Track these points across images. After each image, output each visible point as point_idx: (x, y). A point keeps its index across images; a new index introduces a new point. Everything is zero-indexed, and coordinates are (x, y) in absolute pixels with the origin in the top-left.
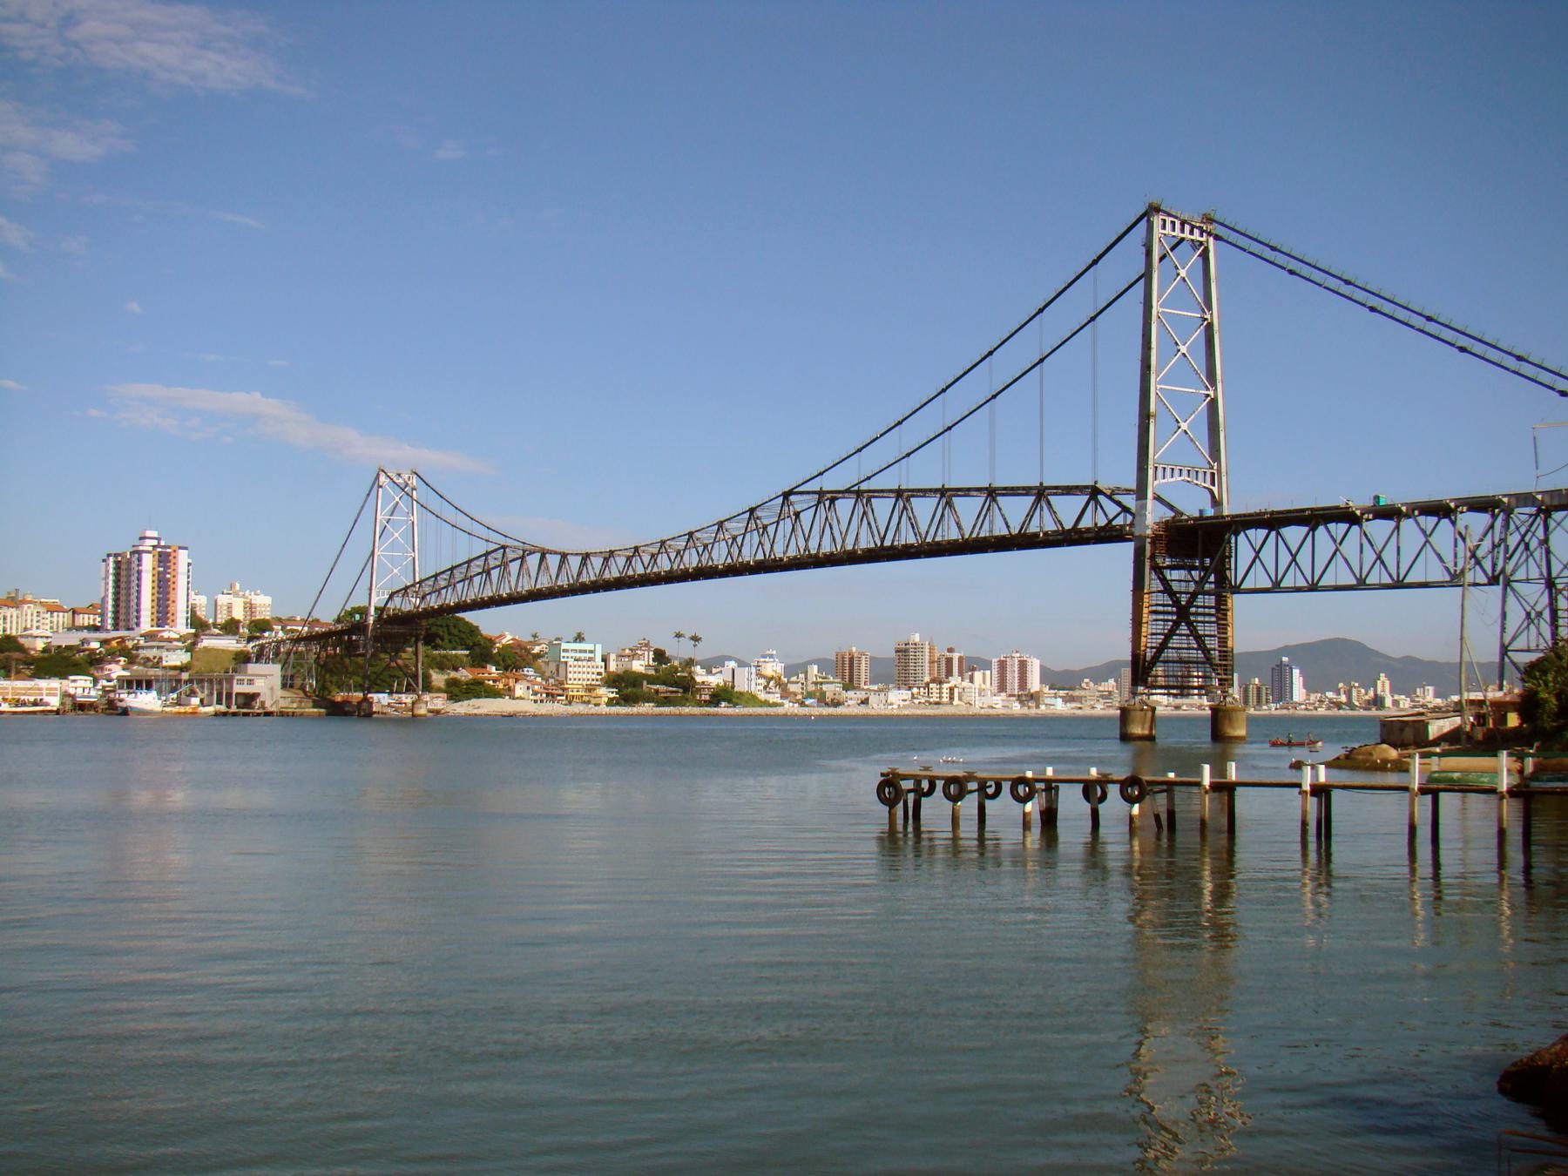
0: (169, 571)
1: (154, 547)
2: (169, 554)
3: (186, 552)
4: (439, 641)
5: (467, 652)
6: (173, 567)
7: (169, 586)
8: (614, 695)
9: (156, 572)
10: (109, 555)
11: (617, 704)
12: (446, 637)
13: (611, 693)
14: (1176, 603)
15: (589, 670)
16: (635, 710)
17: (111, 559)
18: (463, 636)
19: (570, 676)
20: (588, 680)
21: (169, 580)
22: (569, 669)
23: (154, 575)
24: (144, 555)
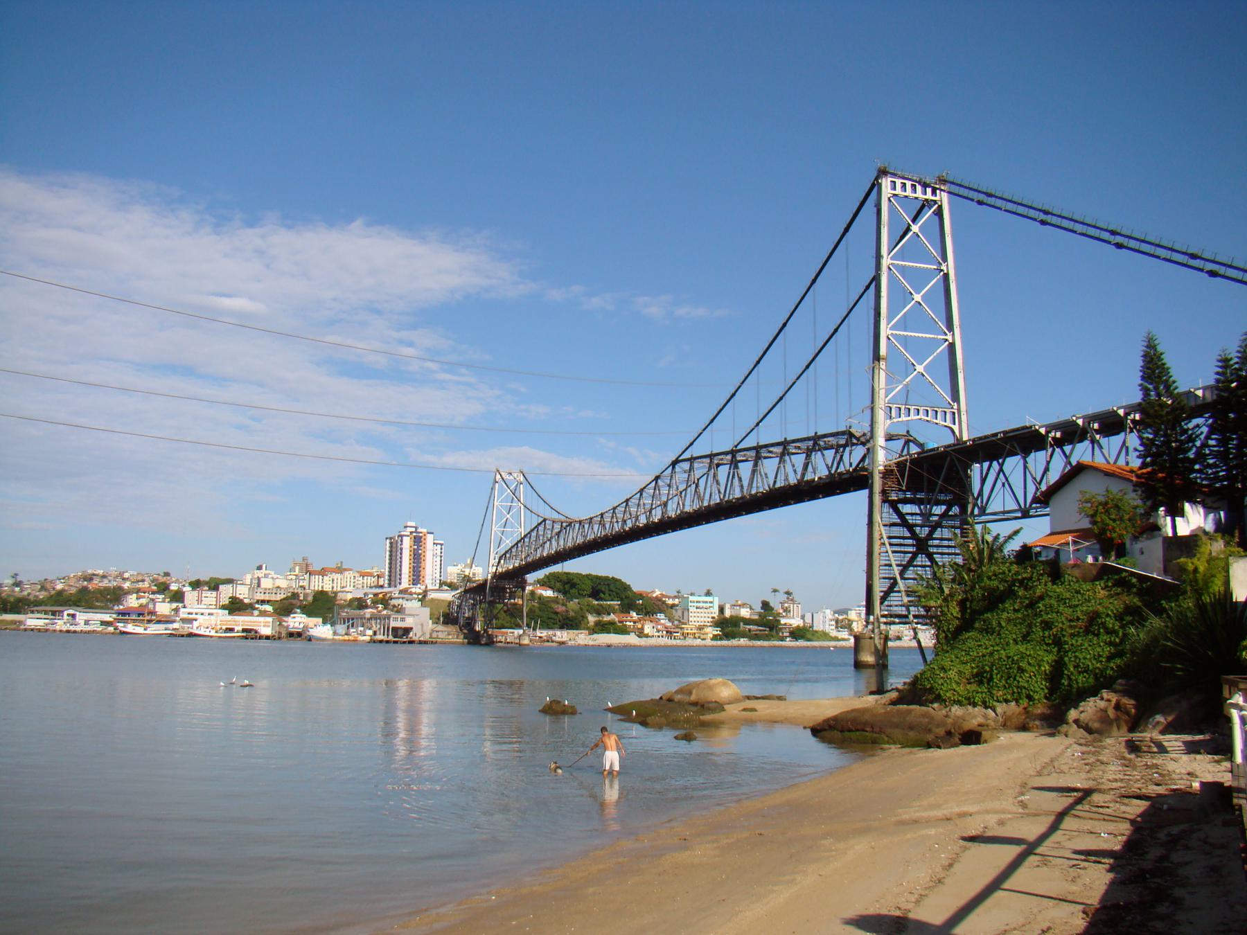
1: (411, 533)
2: (421, 537)
3: (432, 535)
4: (602, 595)
5: (619, 602)
6: (423, 545)
7: (421, 559)
8: (718, 632)
9: (412, 549)
10: (387, 539)
11: (721, 639)
12: (607, 592)
13: (717, 631)
15: (705, 615)
16: (734, 642)
17: (388, 541)
18: (619, 591)
19: (691, 619)
20: (705, 622)
21: (421, 554)
22: (690, 614)
23: (411, 551)
24: (404, 538)
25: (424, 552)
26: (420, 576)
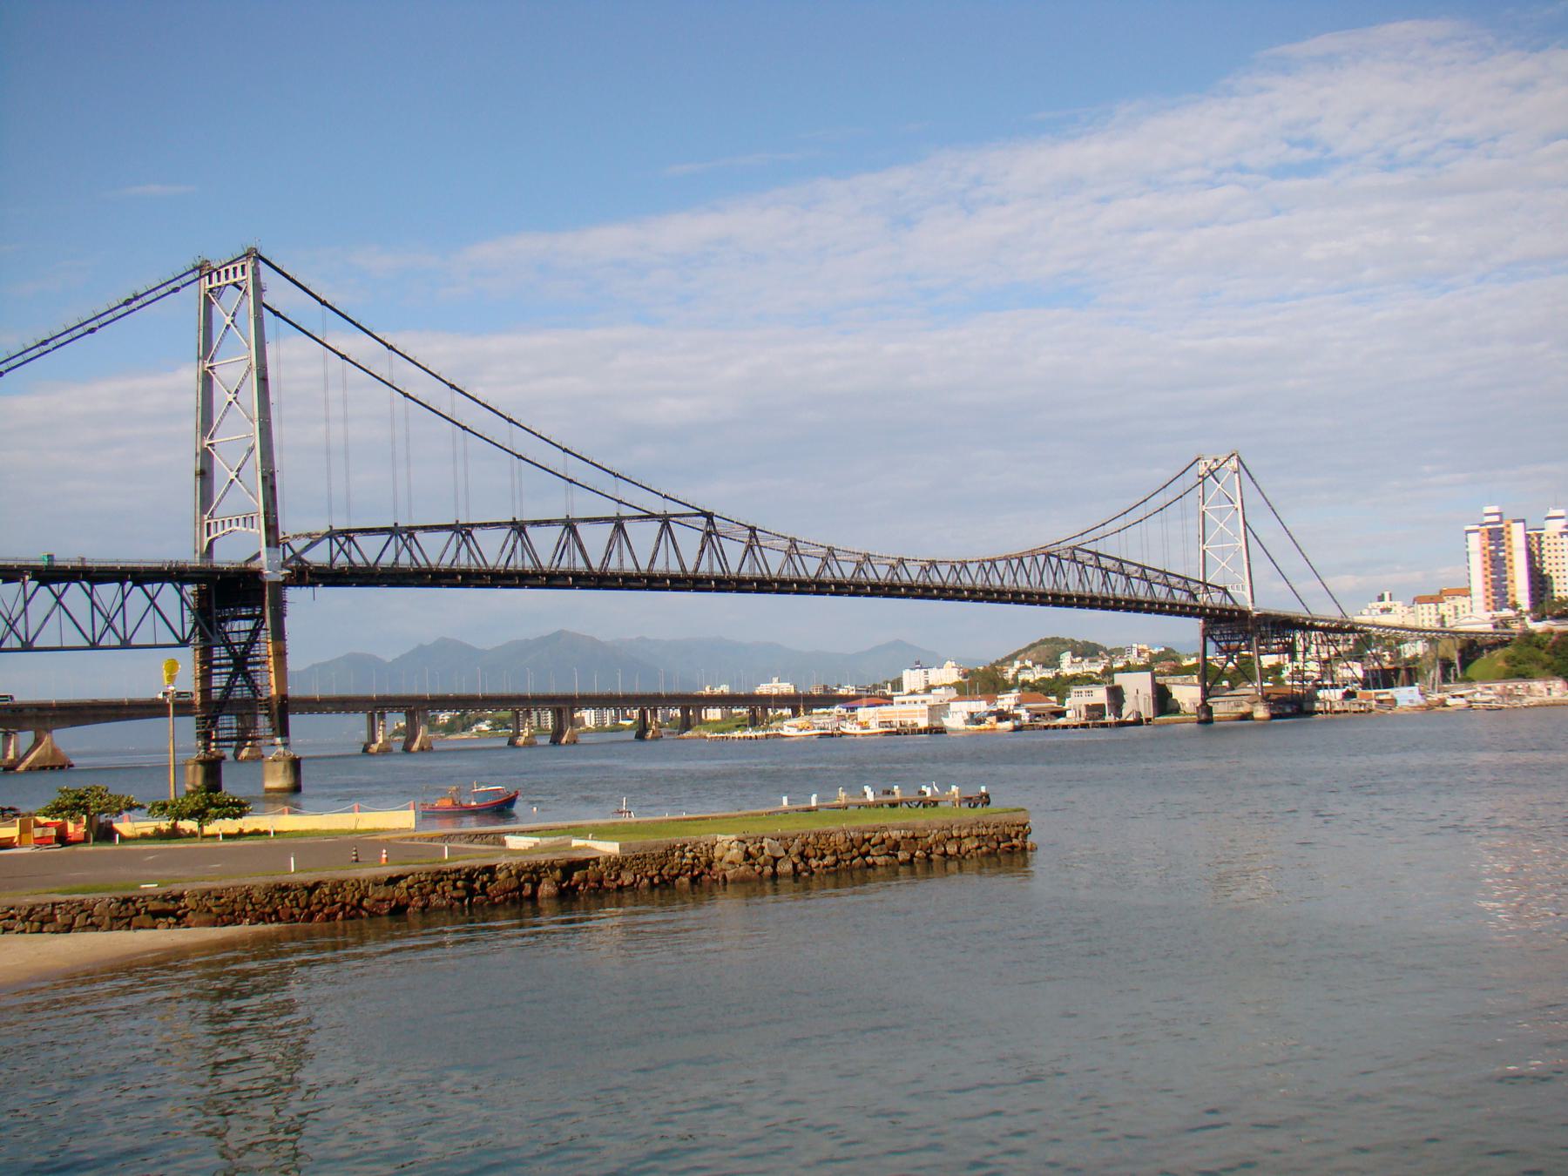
0: (1503, 548)
2: (1502, 530)
6: (1507, 543)
7: (1505, 565)
9: (1486, 552)
14: (233, 655)
21: (1504, 558)
23: (1485, 555)
25: (1510, 554)
26: (1506, 594)
